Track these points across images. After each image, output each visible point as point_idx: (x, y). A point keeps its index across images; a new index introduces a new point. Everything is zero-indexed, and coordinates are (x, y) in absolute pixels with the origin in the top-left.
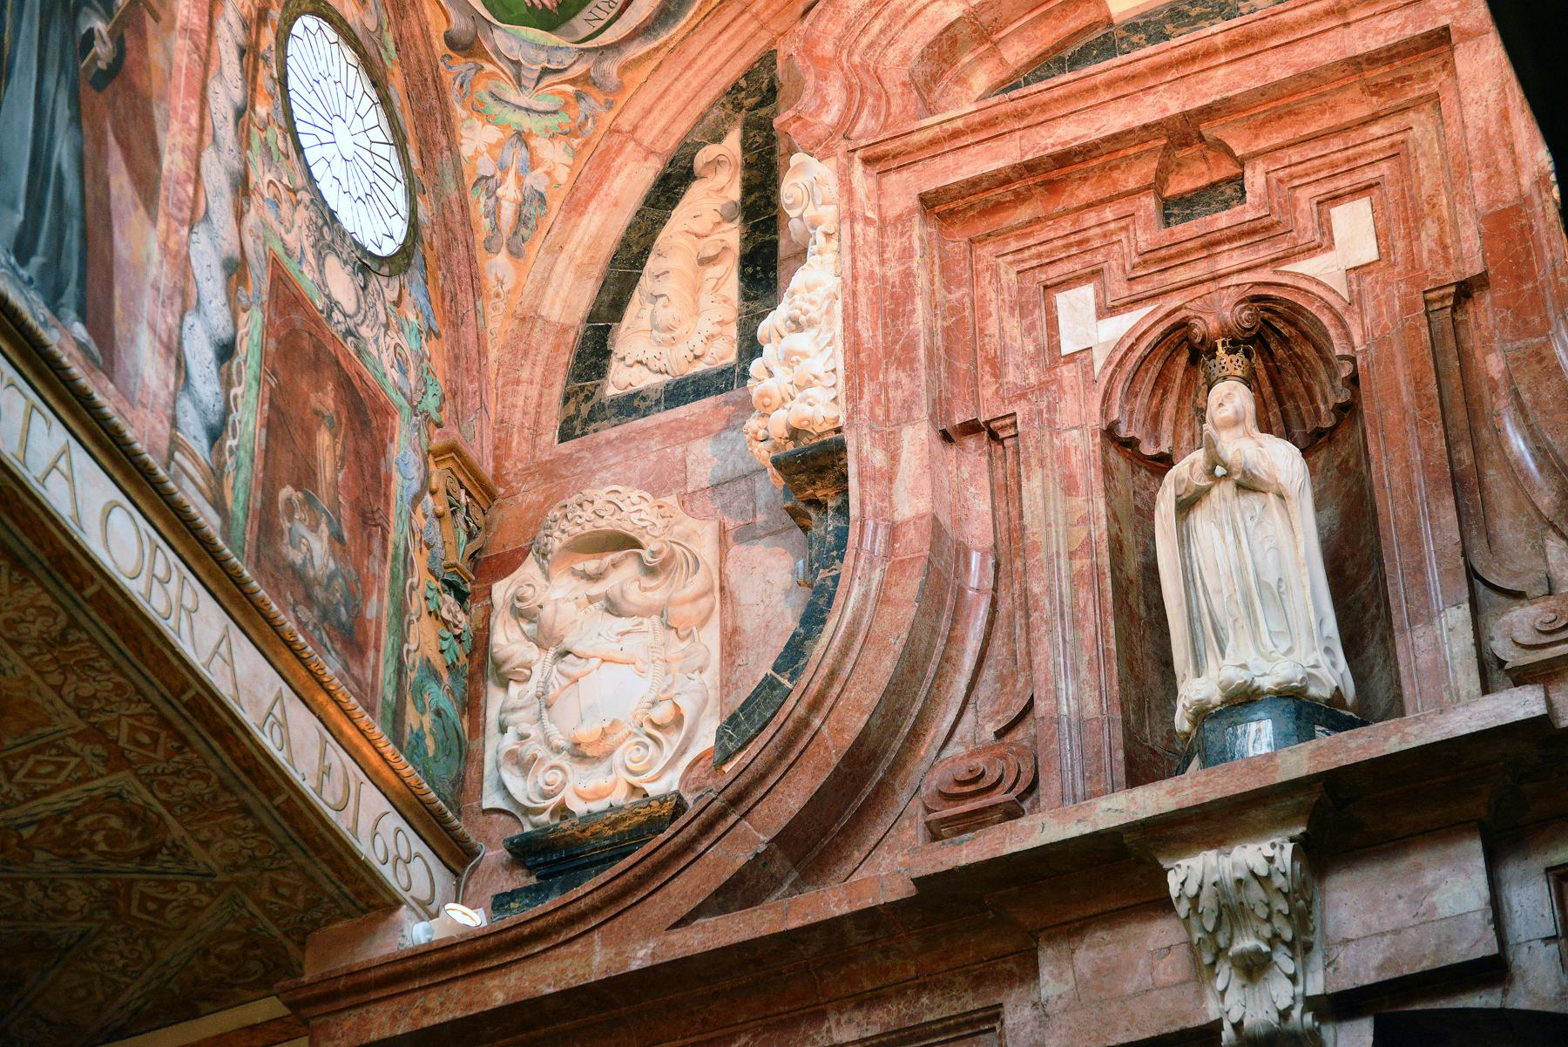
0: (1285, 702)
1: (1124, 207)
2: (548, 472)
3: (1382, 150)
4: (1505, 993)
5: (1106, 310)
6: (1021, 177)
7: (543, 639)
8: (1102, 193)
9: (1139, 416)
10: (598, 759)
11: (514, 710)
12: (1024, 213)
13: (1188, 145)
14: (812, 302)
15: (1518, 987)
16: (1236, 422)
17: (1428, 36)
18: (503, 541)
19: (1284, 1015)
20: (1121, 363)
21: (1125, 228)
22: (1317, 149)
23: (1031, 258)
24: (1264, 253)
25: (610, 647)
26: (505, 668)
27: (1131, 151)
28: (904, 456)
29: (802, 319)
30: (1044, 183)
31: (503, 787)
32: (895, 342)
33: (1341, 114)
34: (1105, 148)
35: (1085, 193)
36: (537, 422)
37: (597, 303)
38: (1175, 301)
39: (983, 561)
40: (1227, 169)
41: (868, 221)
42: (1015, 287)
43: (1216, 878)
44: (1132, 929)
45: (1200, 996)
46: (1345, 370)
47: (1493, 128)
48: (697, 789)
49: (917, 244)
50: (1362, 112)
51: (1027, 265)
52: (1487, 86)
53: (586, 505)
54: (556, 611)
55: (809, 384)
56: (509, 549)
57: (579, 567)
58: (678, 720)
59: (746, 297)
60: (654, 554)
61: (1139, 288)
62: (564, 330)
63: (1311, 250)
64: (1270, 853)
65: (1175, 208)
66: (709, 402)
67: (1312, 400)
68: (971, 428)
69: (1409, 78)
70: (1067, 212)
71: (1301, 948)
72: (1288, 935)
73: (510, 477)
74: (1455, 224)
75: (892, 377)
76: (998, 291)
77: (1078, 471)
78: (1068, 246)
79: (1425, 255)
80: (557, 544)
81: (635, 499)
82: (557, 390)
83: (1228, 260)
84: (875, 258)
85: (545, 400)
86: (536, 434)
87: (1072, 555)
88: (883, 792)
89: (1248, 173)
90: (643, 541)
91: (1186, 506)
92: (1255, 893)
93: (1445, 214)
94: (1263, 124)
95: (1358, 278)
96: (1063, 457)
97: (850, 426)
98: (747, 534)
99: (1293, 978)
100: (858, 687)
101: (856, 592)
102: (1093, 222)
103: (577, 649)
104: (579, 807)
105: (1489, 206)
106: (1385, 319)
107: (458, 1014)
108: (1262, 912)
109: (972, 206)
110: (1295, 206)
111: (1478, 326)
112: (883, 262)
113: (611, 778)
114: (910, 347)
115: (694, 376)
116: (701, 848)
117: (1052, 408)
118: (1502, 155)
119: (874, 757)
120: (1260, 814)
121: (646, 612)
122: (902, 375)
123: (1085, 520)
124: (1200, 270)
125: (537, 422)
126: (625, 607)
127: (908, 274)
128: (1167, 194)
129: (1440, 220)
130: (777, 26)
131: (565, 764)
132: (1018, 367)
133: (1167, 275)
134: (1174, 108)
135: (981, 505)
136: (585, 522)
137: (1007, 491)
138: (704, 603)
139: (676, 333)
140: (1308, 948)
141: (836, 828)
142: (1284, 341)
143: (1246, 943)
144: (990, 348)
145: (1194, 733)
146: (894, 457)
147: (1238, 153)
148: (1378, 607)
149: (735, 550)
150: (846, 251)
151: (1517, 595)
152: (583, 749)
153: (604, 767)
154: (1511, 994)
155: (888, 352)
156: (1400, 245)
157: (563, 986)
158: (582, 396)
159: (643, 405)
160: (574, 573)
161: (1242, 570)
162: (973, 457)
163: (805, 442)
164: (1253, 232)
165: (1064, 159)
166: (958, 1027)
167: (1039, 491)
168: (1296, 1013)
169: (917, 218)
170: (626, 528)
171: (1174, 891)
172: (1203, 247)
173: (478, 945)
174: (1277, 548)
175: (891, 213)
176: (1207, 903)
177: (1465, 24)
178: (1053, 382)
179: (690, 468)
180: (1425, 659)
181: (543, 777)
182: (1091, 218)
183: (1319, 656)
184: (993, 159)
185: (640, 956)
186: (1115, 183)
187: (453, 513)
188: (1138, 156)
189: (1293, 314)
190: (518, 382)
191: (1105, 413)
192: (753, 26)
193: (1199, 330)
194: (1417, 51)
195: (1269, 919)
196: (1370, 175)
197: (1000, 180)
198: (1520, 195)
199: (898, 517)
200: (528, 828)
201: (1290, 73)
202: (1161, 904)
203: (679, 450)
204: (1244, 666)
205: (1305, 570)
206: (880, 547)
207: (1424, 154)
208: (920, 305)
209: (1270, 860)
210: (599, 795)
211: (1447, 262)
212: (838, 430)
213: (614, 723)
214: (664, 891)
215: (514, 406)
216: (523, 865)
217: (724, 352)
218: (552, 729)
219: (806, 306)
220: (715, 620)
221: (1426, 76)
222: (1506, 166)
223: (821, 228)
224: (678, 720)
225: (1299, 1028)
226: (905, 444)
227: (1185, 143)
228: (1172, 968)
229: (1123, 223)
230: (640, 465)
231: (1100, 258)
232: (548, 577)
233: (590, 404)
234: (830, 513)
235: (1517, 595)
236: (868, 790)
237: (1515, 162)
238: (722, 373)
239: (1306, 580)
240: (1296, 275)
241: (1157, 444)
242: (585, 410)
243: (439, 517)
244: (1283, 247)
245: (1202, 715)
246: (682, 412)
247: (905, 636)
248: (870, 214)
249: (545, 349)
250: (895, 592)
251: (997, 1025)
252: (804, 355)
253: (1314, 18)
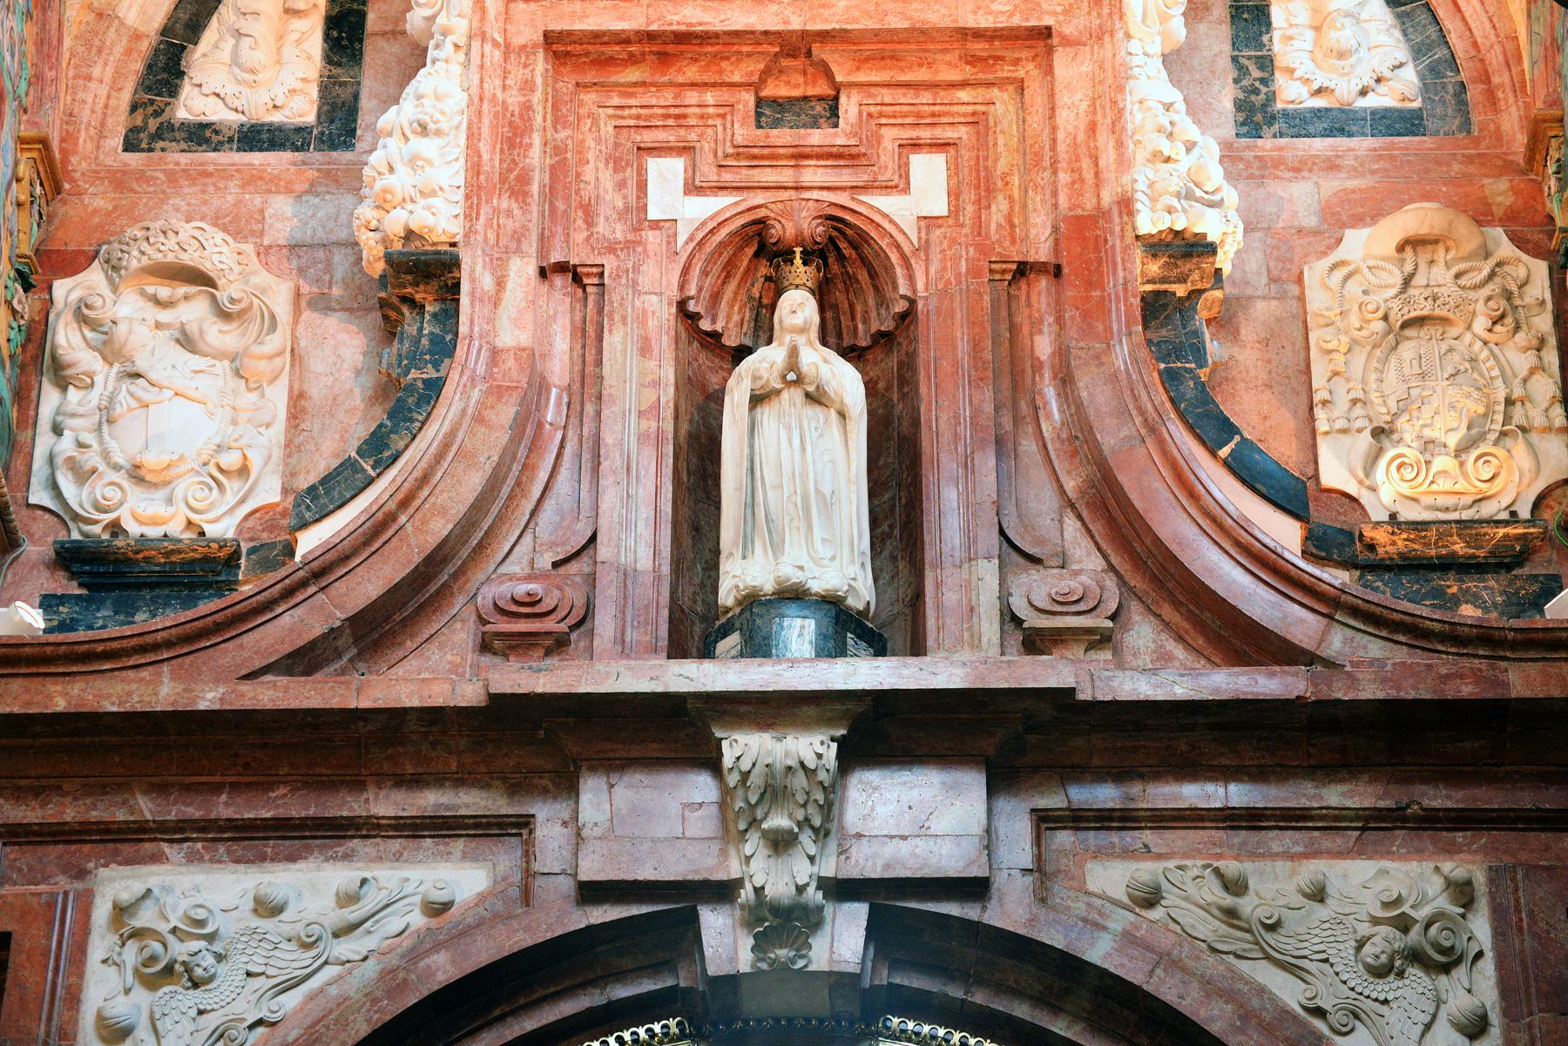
0: (827, 607)
1: (725, 96)
2: (119, 181)
3: (964, 115)
4: (984, 908)
5: (693, 188)
6: (640, 41)
7: (110, 350)
8: (707, 77)
9: (705, 294)
10: (155, 486)
11: (73, 415)
12: (632, 75)
13: (793, 56)
14: (443, 113)
15: (993, 903)
16: (803, 330)
17: (1031, 29)
18: (72, 240)
19: (801, 889)
20: (701, 244)
21: (723, 116)
22: (907, 97)
23: (630, 117)
24: (846, 177)
25: (180, 382)
26: (69, 372)
27: (745, 49)
28: (510, 285)
29: (431, 126)
30: (658, 53)
31: (55, 487)
32: (510, 170)
33: (936, 72)
34: (727, 39)
35: (692, 73)
36: (103, 124)
37: (173, 18)
38: (759, 198)
39: (559, 398)
40: (822, 88)
41: (495, 44)
42: (612, 140)
43: (769, 761)
44: (668, 778)
45: (724, 853)
46: (900, 307)
47: (1081, 137)
48: (252, 539)
49: (539, 80)
50: (954, 75)
51: (625, 123)
52: (1079, 96)
53: (170, 234)
54: (130, 332)
55: (433, 193)
56: (71, 247)
57: (151, 290)
58: (244, 471)
59: (328, 60)
60: (233, 301)
61: (727, 177)
62: (137, 36)
63: (888, 188)
64: (820, 750)
65: (770, 110)
66: (287, 156)
67: (853, 318)
68: (562, 268)
69: (1002, 58)
70: (671, 84)
71: (822, 834)
72: (817, 822)
73: (78, 175)
74: (1024, 206)
75: (505, 204)
76: (598, 141)
77: (653, 336)
78: (667, 116)
79: (993, 227)
80: (134, 264)
81: (218, 241)
82: (126, 97)
83: (813, 174)
84: (498, 82)
85: (112, 102)
86: (101, 136)
87: (640, 414)
88: (444, 593)
89: (843, 99)
90: (220, 283)
91: (757, 400)
92: (800, 781)
93: (1016, 194)
94: (867, 60)
95: (928, 227)
96: (642, 318)
97: (467, 244)
98: (322, 304)
99: (812, 859)
100: (445, 495)
101: (457, 407)
102: (694, 101)
103: (152, 376)
104: (134, 529)
105: (1071, 209)
106: (949, 275)
107: (16, 710)
108: (801, 798)
109: (587, 54)
110: (879, 143)
111: (1029, 305)
112: (504, 88)
113: (171, 510)
114: (524, 179)
115: (270, 124)
116: (279, 610)
117: (636, 269)
118: (1086, 163)
119: (445, 561)
120: (810, 711)
121: (219, 355)
122: (515, 206)
123: (656, 384)
124: (785, 176)
125: (103, 124)
126: (202, 346)
127: (527, 107)
128: (763, 94)
129: (1011, 198)
131: (125, 484)
132: (607, 219)
133: (756, 171)
134: (796, 24)
135: (561, 344)
136: (167, 251)
137: (590, 337)
138: (278, 362)
139: (259, 77)
140: (827, 834)
141: (398, 617)
142: (841, 258)
143: (779, 821)
144: (585, 194)
145: (738, 610)
146: (500, 284)
147: (839, 78)
148: (891, 527)
149: (306, 315)
150: (474, 68)
151: (1035, 560)
152: (143, 472)
153: (161, 494)
154: (989, 911)
155: (503, 180)
156: (970, 209)
157: (127, 707)
158: (150, 110)
159: (215, 138)
160: (143, 293)
161: (804, 475)
162: (559, 299)
163: (414, 246)
164: (839, 156)
165: (684, 38)
166: (489, 826)
167: (619, 348)
168: (811, 890)
169: (541, 55)
170: (207, 267)
171: (728, 761)
172: (793, 157)
173: (49, 650)
174: (833, 462)
175: (518, 41)
176: (756, 780)
177: (1068, 30)
178: (639, 243)
179: (269, 221)
180: (951, 597)
181: (100, 489)
182: (692, 97)
183: (854, 570)
184: (621, 18)
185: (209, 698)
186: (721, 72)
187: (32, 202)
188: (749, 55)
189: (860, 241)
190: (89, 78)
191: (682, 287)
194: (1017, 38)
195: (804, 806)
196: (949, 134)
197: (622, 39)
198: (1098, 207)
199: (499, 343)
200: (76, 536)
201: (906, 25)
202: (713, 765)
203: (258, 200)
204: (801, 568)
205: (854, 488)
206: (481, 369)
207: (1003, 132)
208: (537, 140)
209: (819, 756)
210: (155, 522)
211: (1013, 241)
212: (453, 245)
213: (182, 458)
214: (237, 642)
215: (84, 102)
216: (67, 568)
217: (303, 109)
218: (112, 445)
219: (437, 116)
220: (284, 380)
221: (1016, 62)
222: (1089, 176)
223: (450, 39)
224: (244, 471)
225: (811, 904)
226: (512, 273)
227: (793, 54)
228: (704, 823)
229: (721, 111)
230: (216, 203)
231: (693, 136)
232: (115, 289)
233: (159, 120)
234: (427, 317)
235: (1035, 560)
236: (433, 588)
237: (1097, 174)
238: (299, 130)
239: (854, 496)
240: (872, 207)
241: (714, 322)
242: (153, 125)
243: (19, 205)
244: (862, 178)
245: (752, 601)
246: (256, 158)
247: (495, 458)
248: (500, 39)
249: (118, 50)
250: (490, 414)
251: (525, 832)
252: (429, 162)
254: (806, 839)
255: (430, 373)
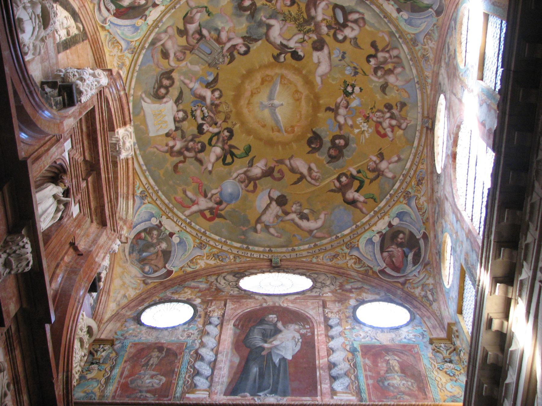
8: (85, 147)
13: (90, 167)
24: (75, 190)
35: (86, 143)
61: (71, 160)
92: (24, 263)
130: (90, 40)
188: (91, 156)
192: (92, 34)
193: (65, 177)
253: (110, 196)
254: (8, 270)
255: (53, 103)
